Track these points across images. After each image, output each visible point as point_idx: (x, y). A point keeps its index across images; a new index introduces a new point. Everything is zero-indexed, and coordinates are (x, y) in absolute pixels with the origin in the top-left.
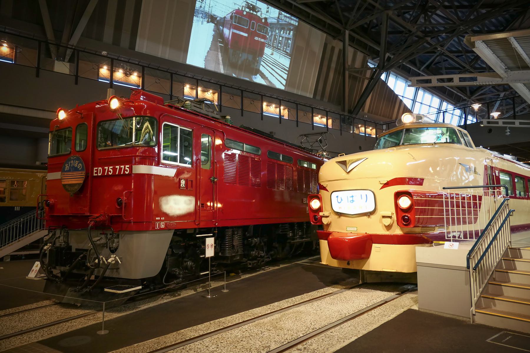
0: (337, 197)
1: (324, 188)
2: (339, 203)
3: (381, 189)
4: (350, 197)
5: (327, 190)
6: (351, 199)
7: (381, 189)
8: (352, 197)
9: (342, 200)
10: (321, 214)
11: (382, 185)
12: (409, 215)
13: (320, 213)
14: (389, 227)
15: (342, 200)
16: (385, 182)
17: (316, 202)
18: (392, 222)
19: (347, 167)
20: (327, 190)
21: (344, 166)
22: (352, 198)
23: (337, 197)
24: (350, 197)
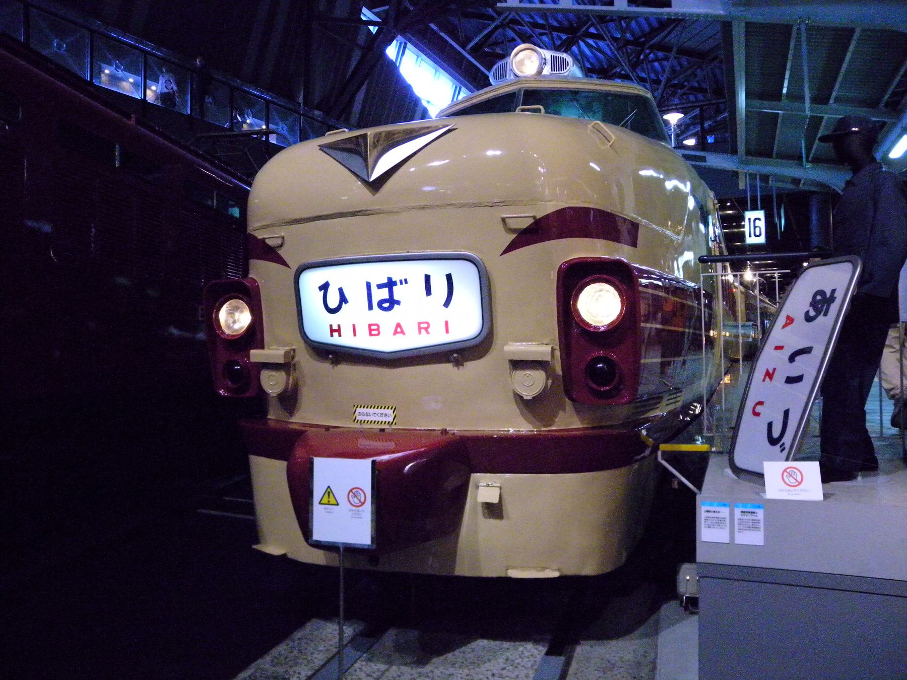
0: (325, 287)
1: (271, 254)
2: (332, 311)
3: (506, 251)
4: (380, 286)
5: (282, 262)
6: (384, 294)
7: (506, 251)
8: (390, 284)
9: (343, 299)
10: (256, 355)
11: (513, 236)
12: (613, 356)
13: (252, 352)
14: (531, 406)
15: (343, 299)
16: (525, 224)
17: (236, 309)
18: (550, 382)
19: (370, 161)
20: (282, 262)
21: (355, 161)
22: (386, 290)
23: (325, 287)
24: (380, 286)
